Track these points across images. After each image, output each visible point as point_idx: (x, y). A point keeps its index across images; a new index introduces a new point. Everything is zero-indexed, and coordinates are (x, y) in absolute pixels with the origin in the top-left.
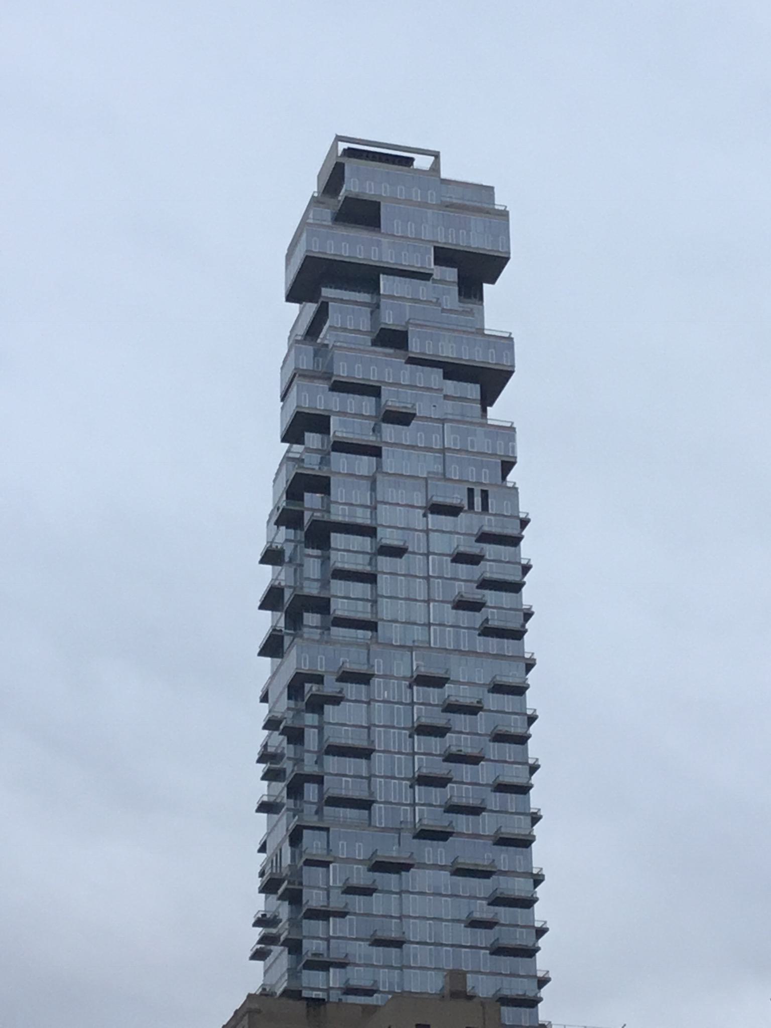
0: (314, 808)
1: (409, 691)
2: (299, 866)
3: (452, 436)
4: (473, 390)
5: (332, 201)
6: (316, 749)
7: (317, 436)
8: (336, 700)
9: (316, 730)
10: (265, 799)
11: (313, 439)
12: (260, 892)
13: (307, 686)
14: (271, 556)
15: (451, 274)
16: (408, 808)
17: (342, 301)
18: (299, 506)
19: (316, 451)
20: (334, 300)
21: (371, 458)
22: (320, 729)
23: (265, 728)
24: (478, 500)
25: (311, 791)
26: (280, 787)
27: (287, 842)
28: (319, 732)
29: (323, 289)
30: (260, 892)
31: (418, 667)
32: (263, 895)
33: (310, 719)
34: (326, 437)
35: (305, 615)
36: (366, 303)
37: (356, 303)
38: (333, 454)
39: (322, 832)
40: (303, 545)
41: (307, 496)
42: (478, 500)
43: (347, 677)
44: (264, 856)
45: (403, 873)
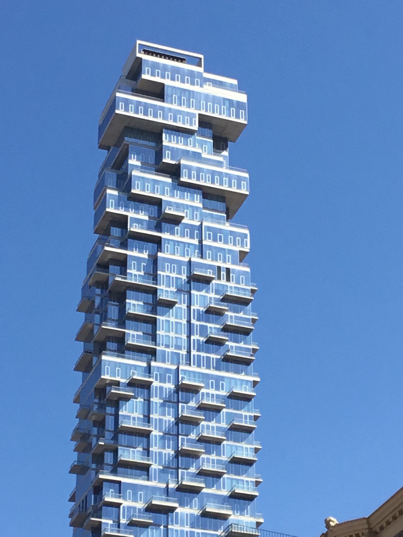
0: (111, 468)
1: (176, 395)
2: (99, 507)
3: (208, 232)
4: (221, 205)
5: (133, 82)
6: (113, 430)
7: (119, 230)
8: (127, 399)
9: (113, 417)
10: (76, 463)
11: (116, 231)
12: (71, 526)
13: (108, 388)
14: (87, 307)
15: (208, 131)
16: (174, 470)
17: (137, 144)
18: (106, 272)
19: (118, 238)
20: (131, 143)
21: (154, 244)
22: (117, 416)
23: (77, 417)
24: (223, 273)
25: (109, 457)
26: (88, 457)
27: (92, 492)
28: (115, 418)
29: (126, 138)
30: (71, 526)
31: (182, 378)
32: (72, 528)
33: (110, 410)
34: (124, 230)
35: (108, 343)
36: (152, 146)
37: (146, 146)
38: (129, 240)
39: (116, 484)
40: (108, 299)
41: (110, 266)
42: (223, 273)
43: (133, 384)
44: (74, 503)
45: (170, 514)
